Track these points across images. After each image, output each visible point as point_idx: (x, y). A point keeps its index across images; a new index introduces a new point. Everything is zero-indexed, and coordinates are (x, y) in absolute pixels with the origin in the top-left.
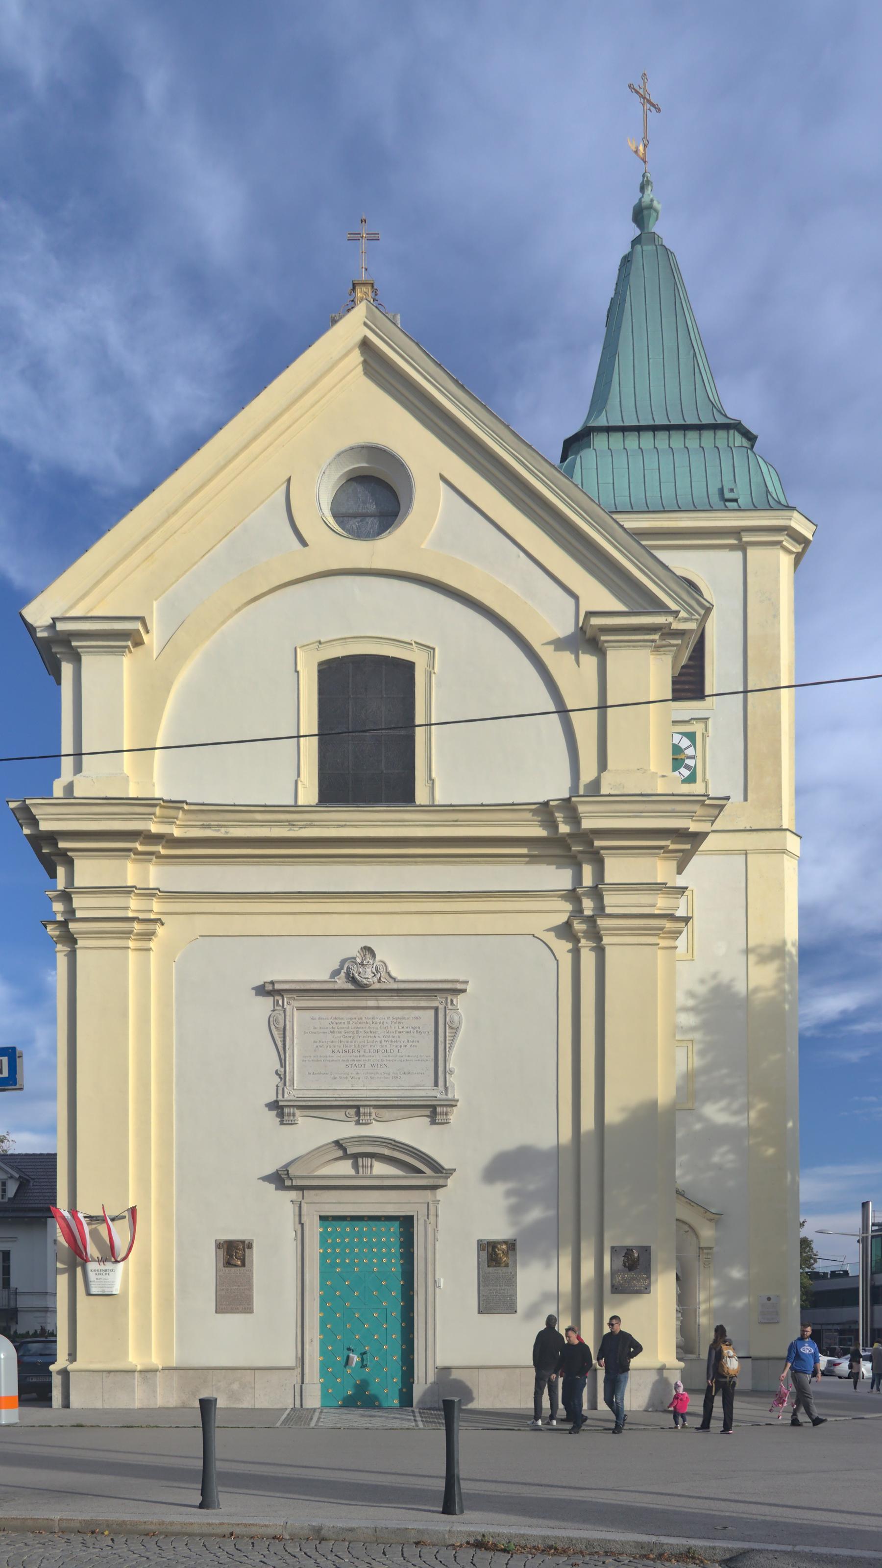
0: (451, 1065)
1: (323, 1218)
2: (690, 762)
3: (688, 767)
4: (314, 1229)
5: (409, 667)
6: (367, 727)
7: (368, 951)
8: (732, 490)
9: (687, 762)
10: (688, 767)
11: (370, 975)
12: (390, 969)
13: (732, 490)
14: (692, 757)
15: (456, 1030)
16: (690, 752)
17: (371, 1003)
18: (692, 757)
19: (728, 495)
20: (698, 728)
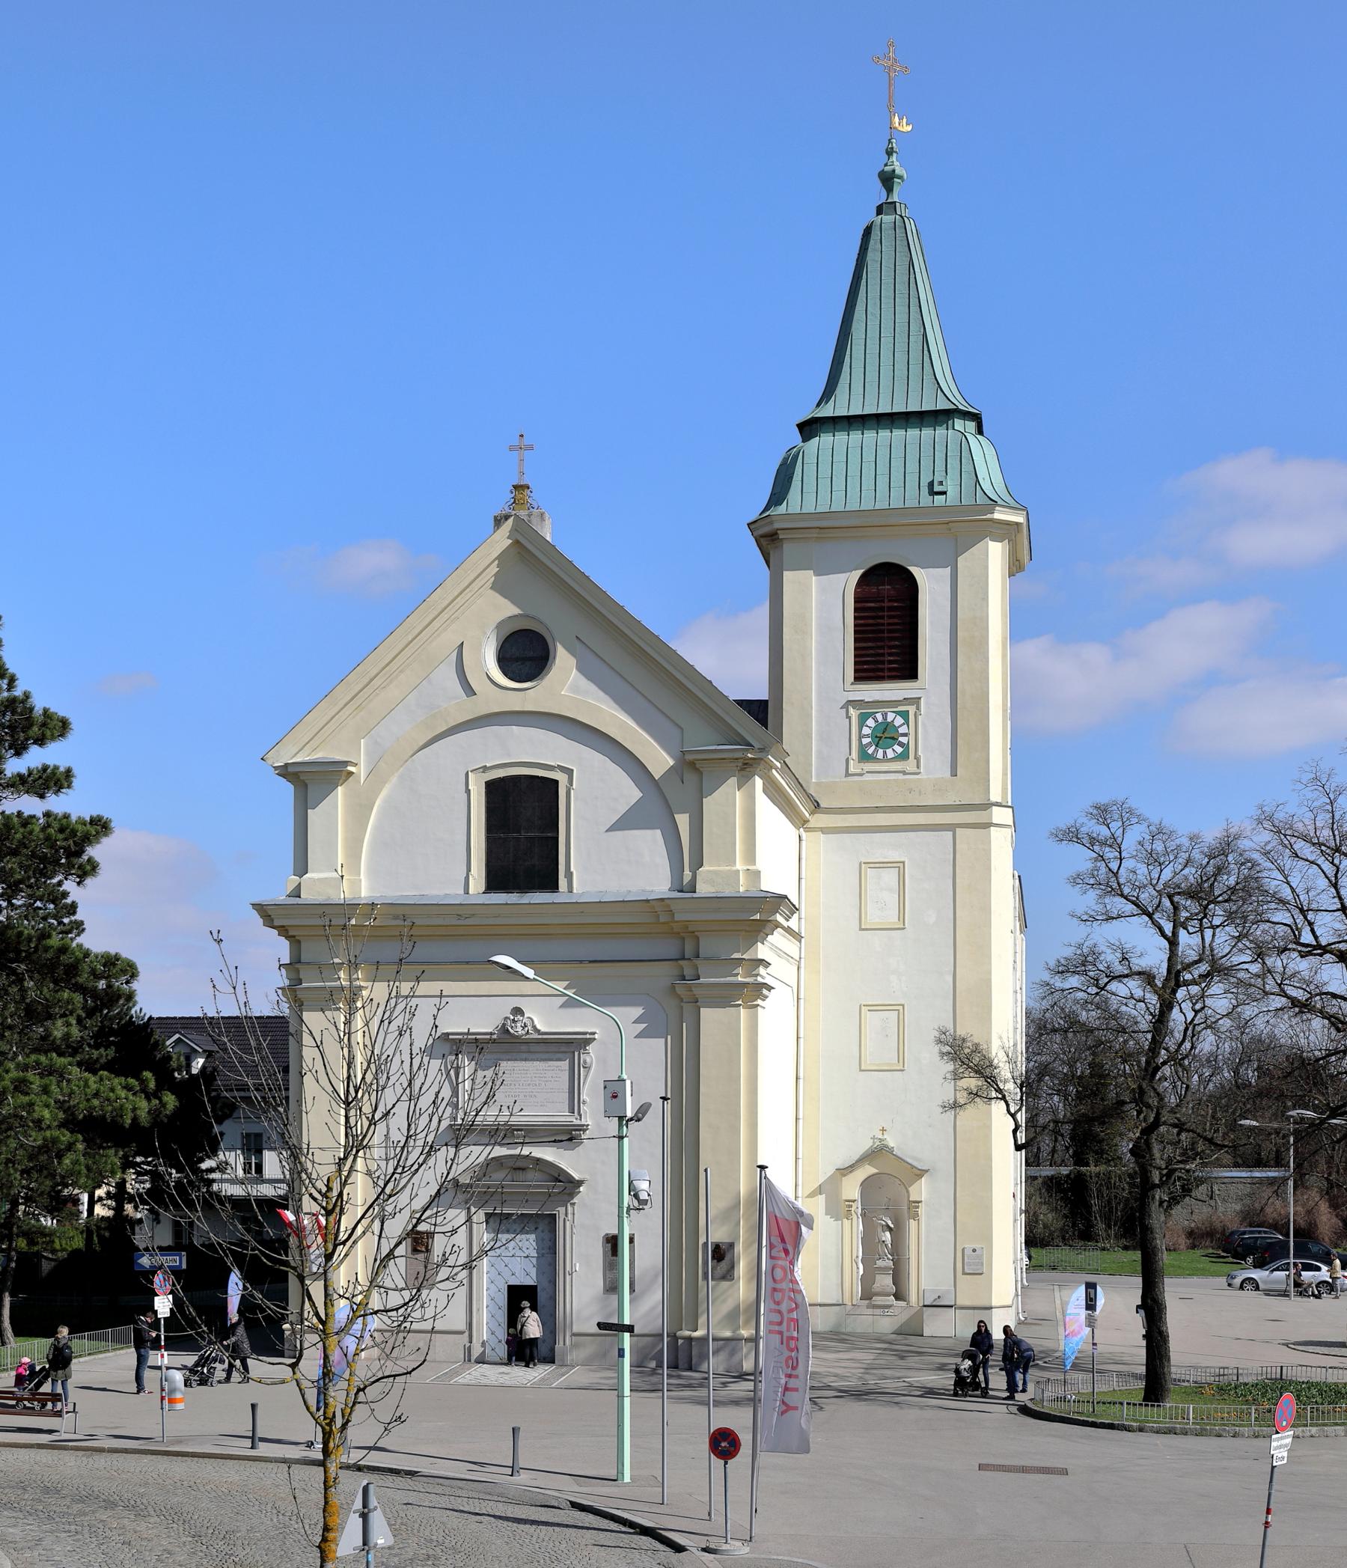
0: (584, 1097)
2: (901, 739)
3: (901, 744)
5: (557, 782)
6: (523, 826)
7: (518, 1011)
8: (941, 483)
9: (901, 739)
10: (901, 744)
11: (519, 1029)
12: (536, 1023)
13: (941, 483)
14: (905, 735)
15: (588, 1068)
18: (905, 735)
19: (937, 488)
20: (912, 709)
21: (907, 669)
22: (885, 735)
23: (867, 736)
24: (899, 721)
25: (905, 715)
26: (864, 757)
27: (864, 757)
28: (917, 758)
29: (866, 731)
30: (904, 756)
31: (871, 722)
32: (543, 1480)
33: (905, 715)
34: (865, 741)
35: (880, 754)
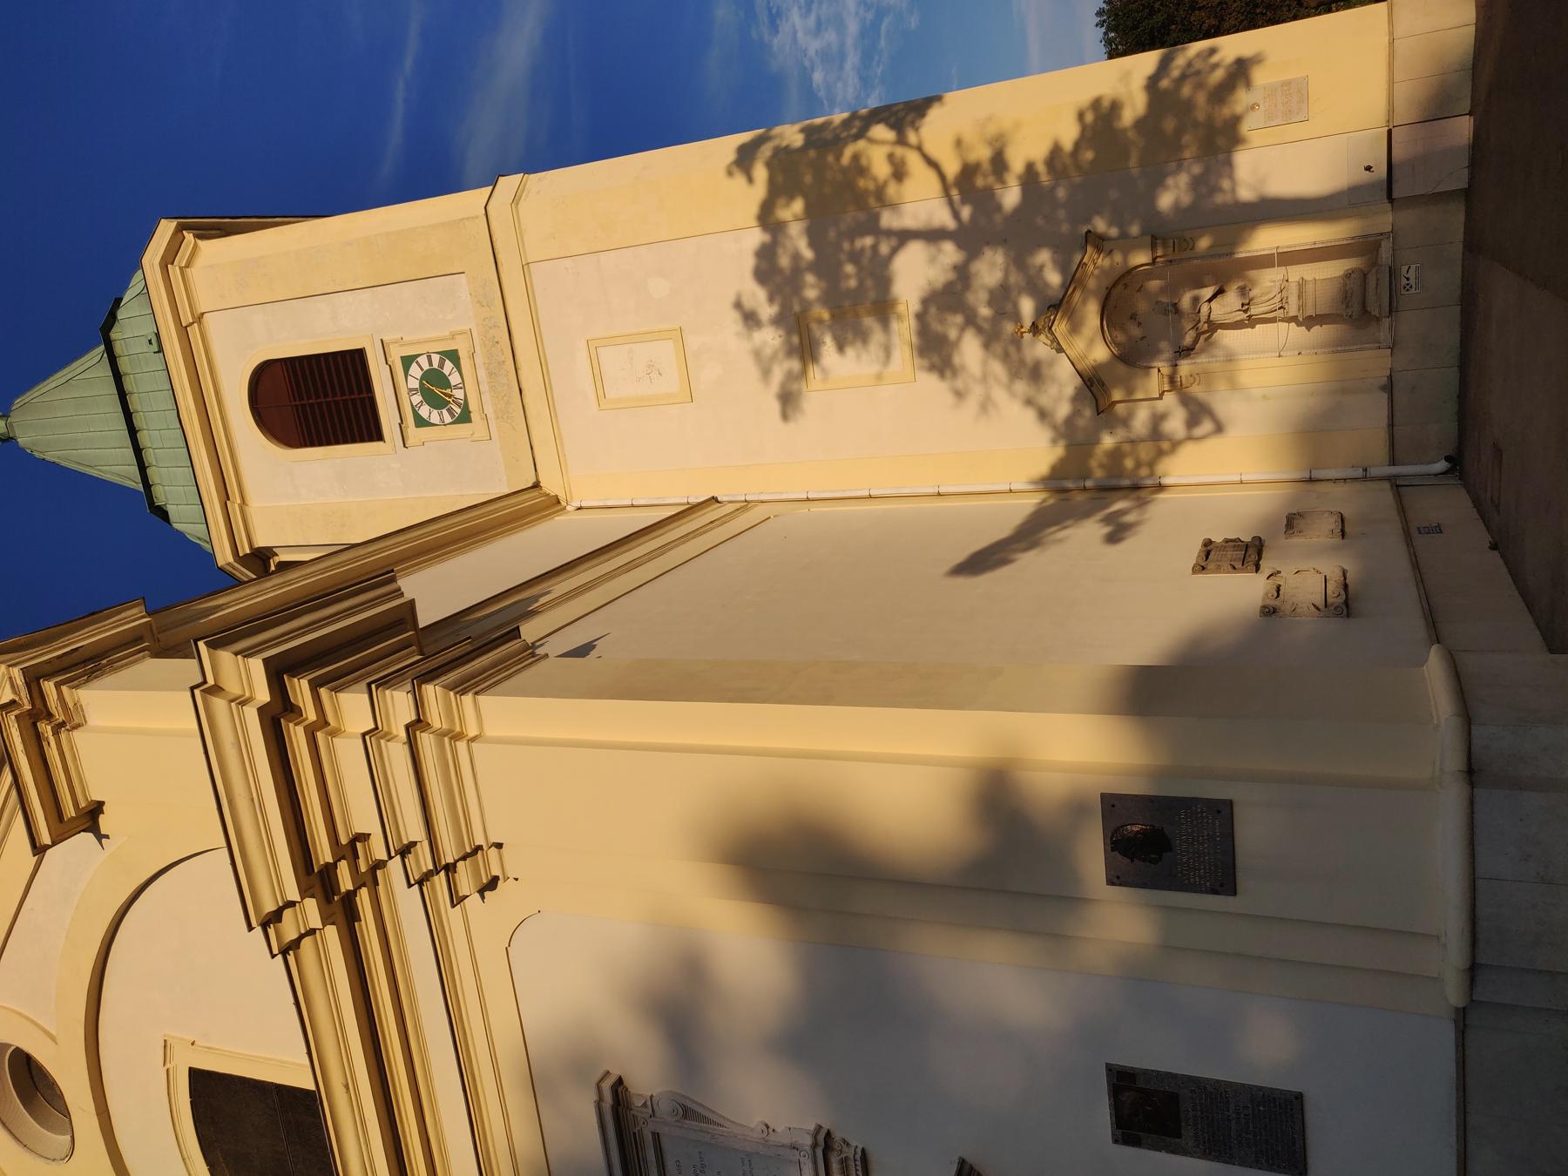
2: (435, 365)
3: (442, 364)
9: (435, 365)
10: (442, 364)
14: (429, 358)
16: (423, 360)
18: (429, 358)
21: (351, 365)
22: (435, 388)
23: (440, 415)
24: (415, 371)
25: (408, 361)
26: (465, 417)
27: (465, 417)
28: (453, 336)
29: (435, 418)
30: (453, 356)
31: (424, 411)
33: (408, 361)
34: (448, 419)
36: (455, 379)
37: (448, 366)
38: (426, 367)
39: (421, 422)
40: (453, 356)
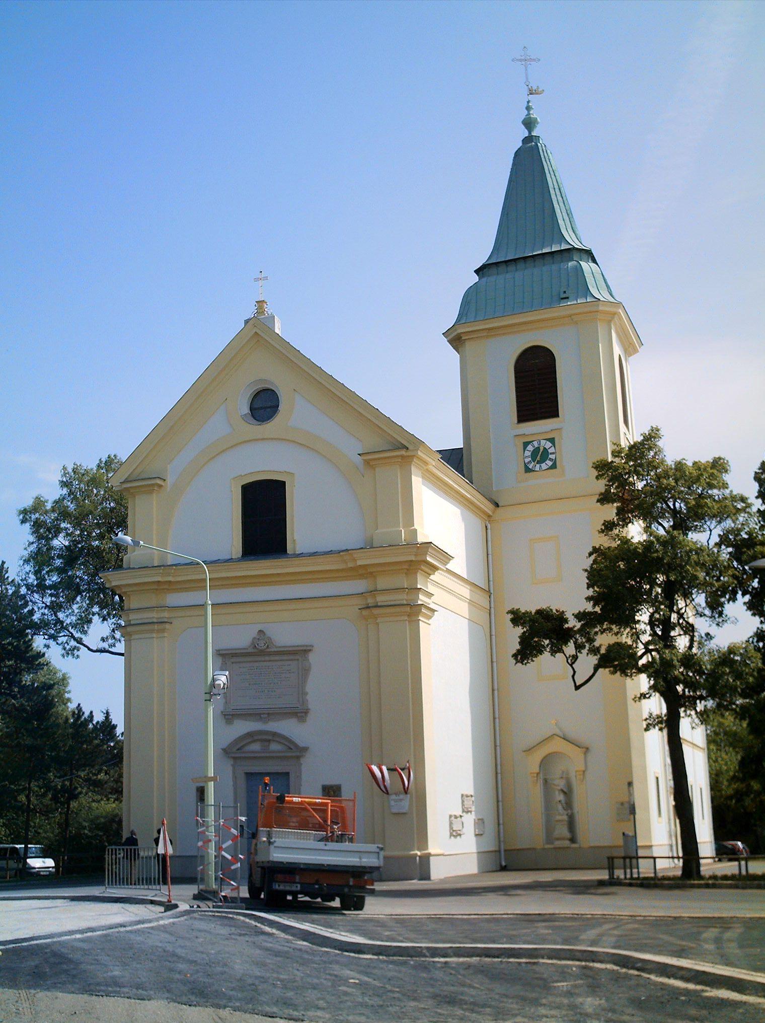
1: (247, 774)
2: (550, 456)
3: (551, 460)
4: (242, 781)
10: (551, 460)
17: (267, 658)
22: (540, 455)
24: (548, 445)
25: (552, 440)
26: (528, 470)
27: (528, 470)
30: (554, 466)
31: (530, 448)
32: (150, 895)
34: (527, 460)
35: (537, 468)
36: (544, 466)
37: (550, 463)
38: (550, 451)
39: (526, 445)
40: (554, 466)
